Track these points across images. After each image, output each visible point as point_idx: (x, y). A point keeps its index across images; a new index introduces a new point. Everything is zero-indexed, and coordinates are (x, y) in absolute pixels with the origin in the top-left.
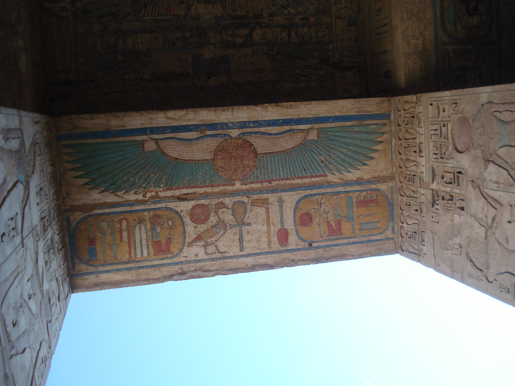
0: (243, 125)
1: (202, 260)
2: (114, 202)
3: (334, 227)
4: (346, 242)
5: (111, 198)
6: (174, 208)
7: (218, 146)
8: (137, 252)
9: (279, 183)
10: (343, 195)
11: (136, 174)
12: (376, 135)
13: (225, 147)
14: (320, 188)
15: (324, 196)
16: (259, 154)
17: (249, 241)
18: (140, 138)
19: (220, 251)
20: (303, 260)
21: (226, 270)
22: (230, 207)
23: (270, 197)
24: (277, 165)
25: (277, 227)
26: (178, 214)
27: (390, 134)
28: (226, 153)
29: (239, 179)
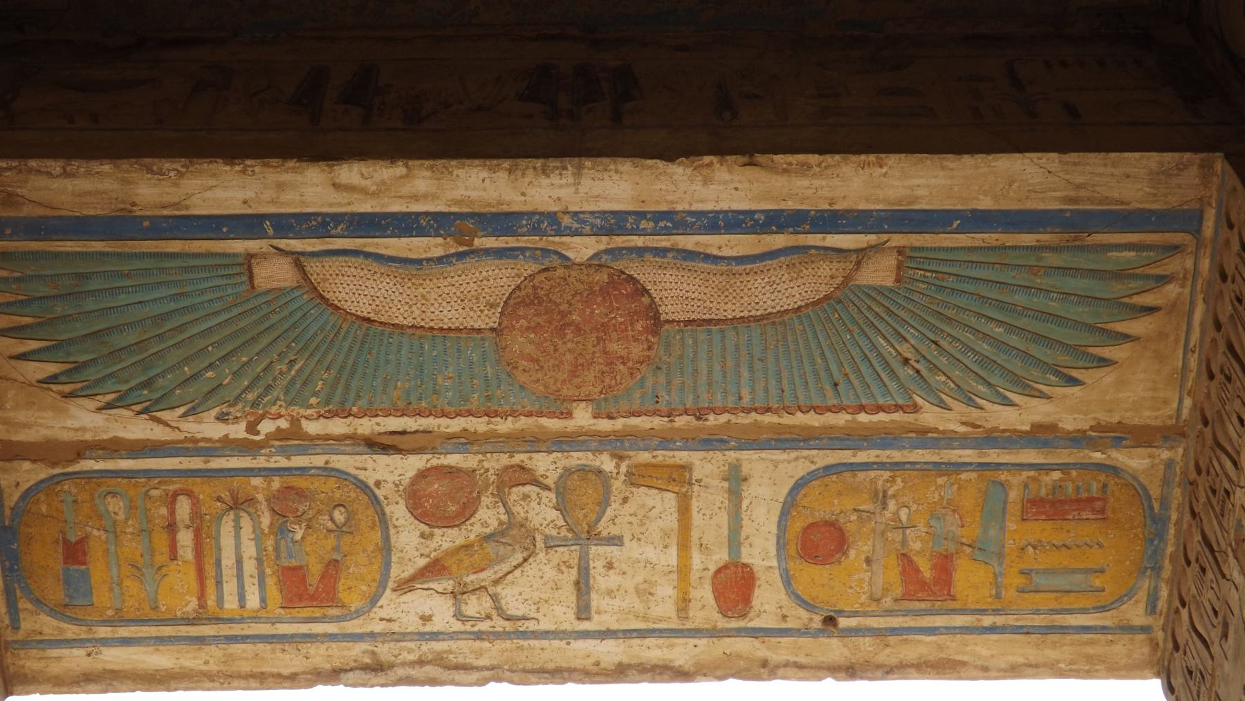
0: (613, 223)
3: (927, 572)
4: (967, 625)
5: (137, 429)
6: (354, 472)
7: (518, 288)
8: (225, 592)
10: (973, 475)
11: (223, 359)
14: (884, 447)
15: (898, 473)
16: (667, 321)
17: (610, 593)
18: (239, 246)
19: (509, 612)
20: (800, 666)
21: (525, 671)
22: (550, 482)
23: (697, 463)
26: (368, 491)
27: (1189, 283)
28: (546, 313)
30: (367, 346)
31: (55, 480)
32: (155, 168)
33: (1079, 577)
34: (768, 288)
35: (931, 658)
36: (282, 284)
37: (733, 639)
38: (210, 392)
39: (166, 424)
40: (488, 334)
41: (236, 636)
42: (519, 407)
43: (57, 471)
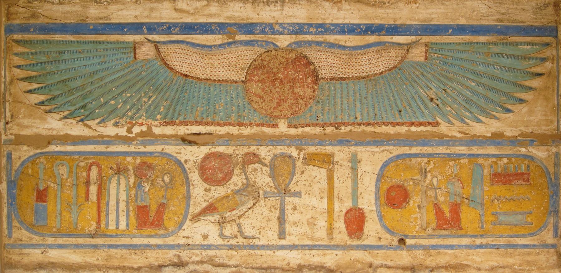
1: (213, 245)
2: (81, 136)
3: (448, 215)
4: (468, 244)
5: (77, 130)
7: (255, 60)
9: (353, 130)
10: (466, 161)
11: (119, 95)
12: (531, 62)
13: (265, 63)
14: (424, 144)
15: (431, 159)
16: (322, 78)
17: (295, 224)
18: (131, 38)
19: (246, 234)
21: (252, 268)
22: (267, 162)
23: (336, 153)
24: (351, 99)
25: (346, 204)
26: (181, 165)
27: (555, 62)
28: (267, 73)
29: (285, 117)
30: (185, 89)
33: (520, 217)
34: (367, 62)
35: (452, 263)
36: (148, 57)
37: (355, 251)
38: (111, 111)
39: (90, 128)
40: (241, 85)
42: (253, 122)
43: (39, 151)
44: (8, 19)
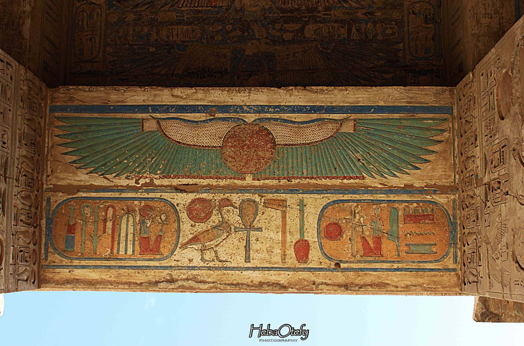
0: (261, 109)
1: (196, 267)
4: (388, 268)
5: (99, 181)
6: (170, 200)
7: (229, 131)
10: (386, 205)
15: (359, 204)
16: (278, 144)
18: (140, 116)
19: (221, 259)
21: (225, 284)
22: (237, 205)
23: (289, 199)
24: (299, 160)
25: (295, 237)
26: (174, 207)
27: (452, 132)
30: (178, 152)
31: (69, 200)
32: (117, 89)
35: (376, 282)
41: (122, 266)
43: (70, 197)
44: (52, 102)
